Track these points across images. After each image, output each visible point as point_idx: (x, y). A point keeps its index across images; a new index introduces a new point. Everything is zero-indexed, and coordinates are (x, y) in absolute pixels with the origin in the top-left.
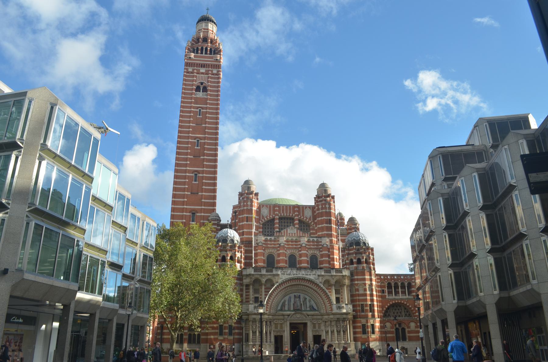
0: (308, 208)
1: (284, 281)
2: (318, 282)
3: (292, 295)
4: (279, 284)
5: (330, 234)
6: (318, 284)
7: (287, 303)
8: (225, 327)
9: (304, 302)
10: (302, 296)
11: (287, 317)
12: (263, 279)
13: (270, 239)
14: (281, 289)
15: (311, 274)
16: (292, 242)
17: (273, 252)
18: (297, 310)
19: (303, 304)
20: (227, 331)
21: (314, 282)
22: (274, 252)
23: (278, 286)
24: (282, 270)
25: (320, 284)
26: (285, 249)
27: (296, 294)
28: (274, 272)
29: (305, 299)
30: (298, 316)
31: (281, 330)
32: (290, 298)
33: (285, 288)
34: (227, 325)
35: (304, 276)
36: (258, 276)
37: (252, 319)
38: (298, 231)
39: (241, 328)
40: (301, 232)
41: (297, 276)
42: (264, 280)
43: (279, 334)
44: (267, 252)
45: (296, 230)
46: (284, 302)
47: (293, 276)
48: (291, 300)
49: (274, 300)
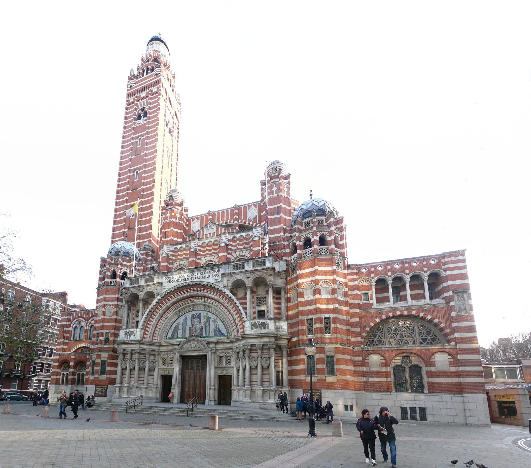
0: (253, 207)
1: (169, 291)
2: (220, 286)
3: (189, 315)
4: (162, 297)
5: (277, 229)
6: (221, 290)
7: (180, 327)
8: (98, 363)
9: (205, 323)
10: (204, 314)
11: (177, 347)
12: (141, 293)
13: (182, 247)
14: (167, 305)
15: (211, 275)
16: (210, 246)
17: (183, 264)
18: (195, 336)
19: (204, 327)
20: (98, 368)
21: (214, 287)
22: (185, 264)
23: (159, 300)
24: (167, 276)
25: (224, 290)
26: (199, 257)
27: (194, 313)
28: (156, 280)
29: (208, 319)
30: (193, 346)
31: (169, 367)
32: (186, 319)
33: (175, 303)
34: (99, 361)
35: (198, 280)
36: (135, 290)
37: (122, 351)
38: (219, 228)
39: (115, 365)
40: (223, 229)
41: (188, 281)
42: (141, 295)
43: (166, 373)
44: (176, 265)
45: (215, 227)
46: (177, 326)
47: (182, 282)
48: (186, 323)
49: (159, 323)
